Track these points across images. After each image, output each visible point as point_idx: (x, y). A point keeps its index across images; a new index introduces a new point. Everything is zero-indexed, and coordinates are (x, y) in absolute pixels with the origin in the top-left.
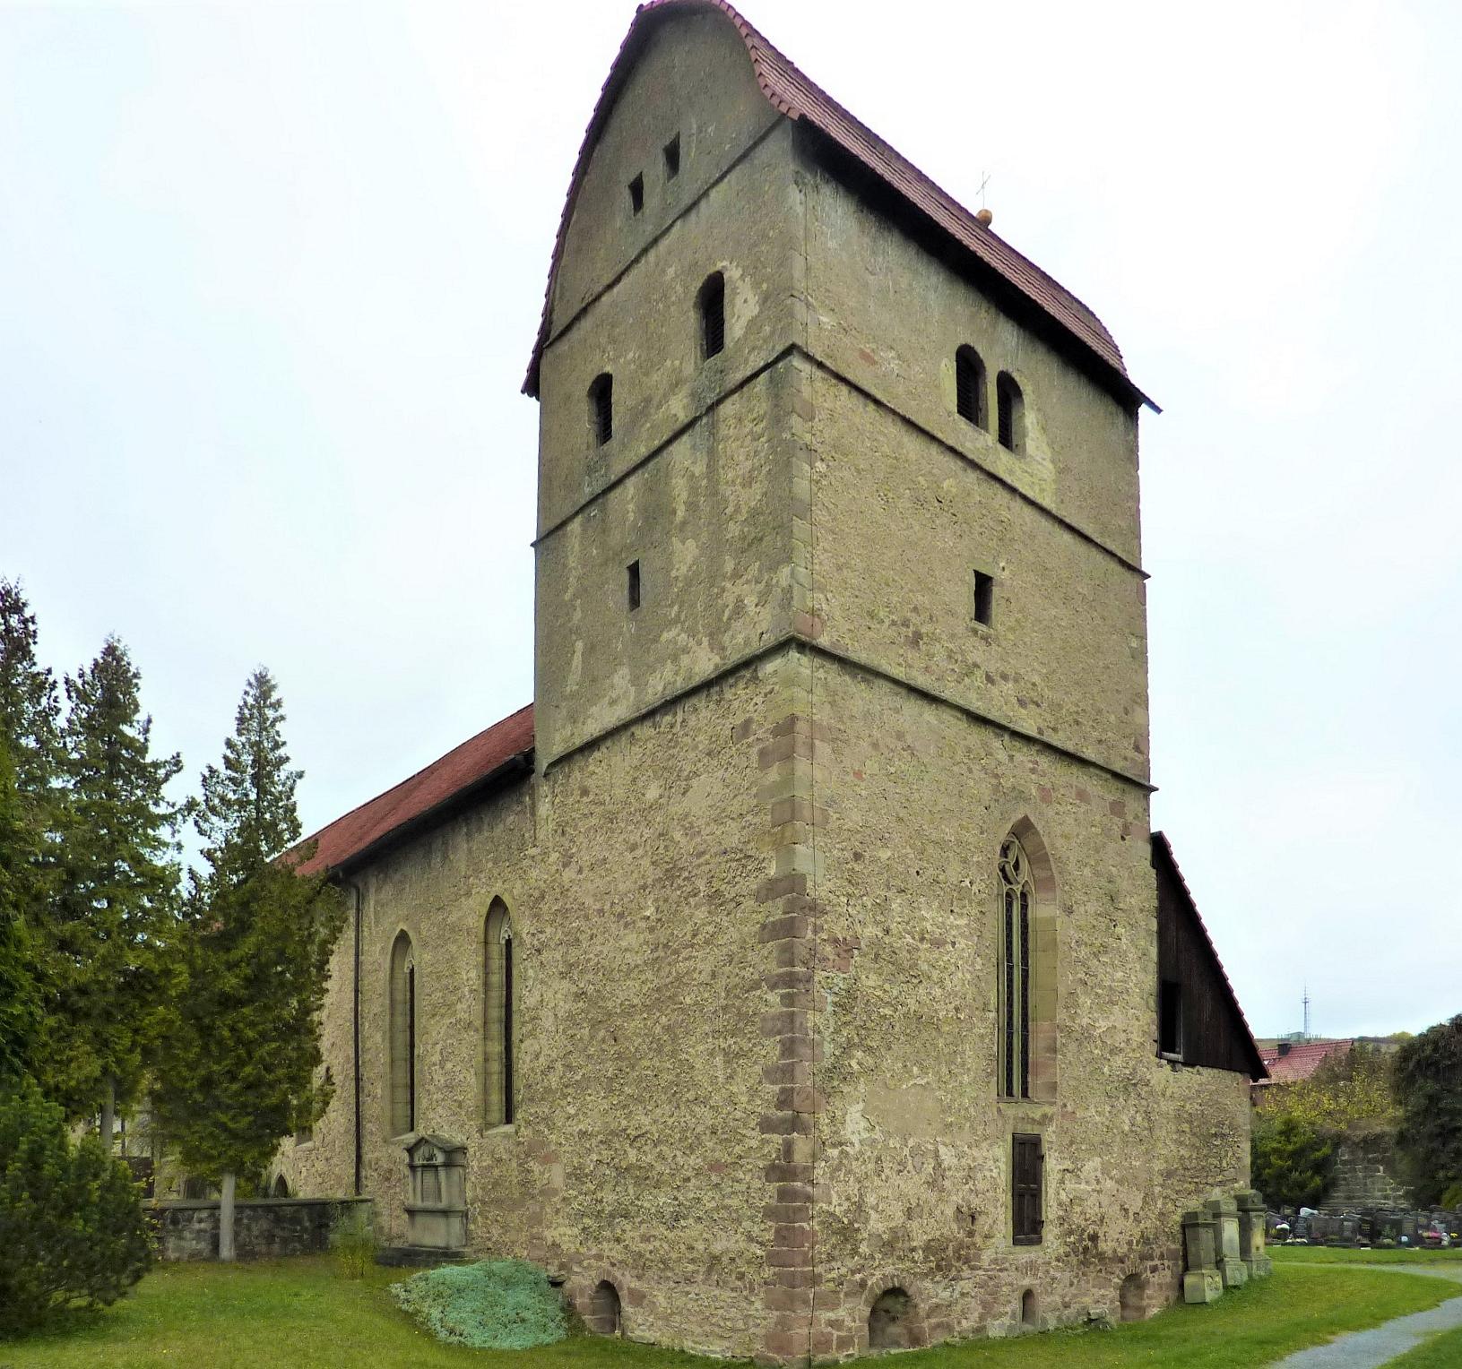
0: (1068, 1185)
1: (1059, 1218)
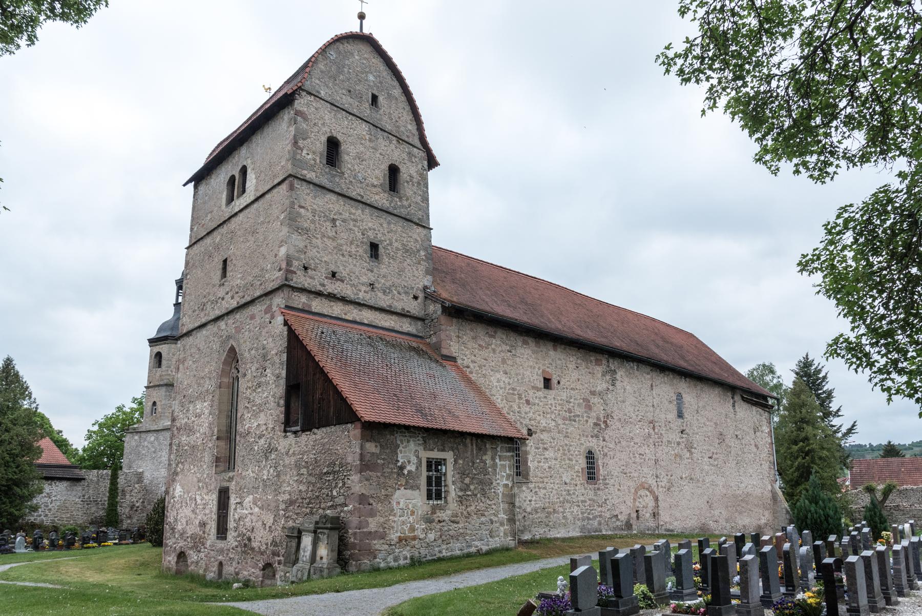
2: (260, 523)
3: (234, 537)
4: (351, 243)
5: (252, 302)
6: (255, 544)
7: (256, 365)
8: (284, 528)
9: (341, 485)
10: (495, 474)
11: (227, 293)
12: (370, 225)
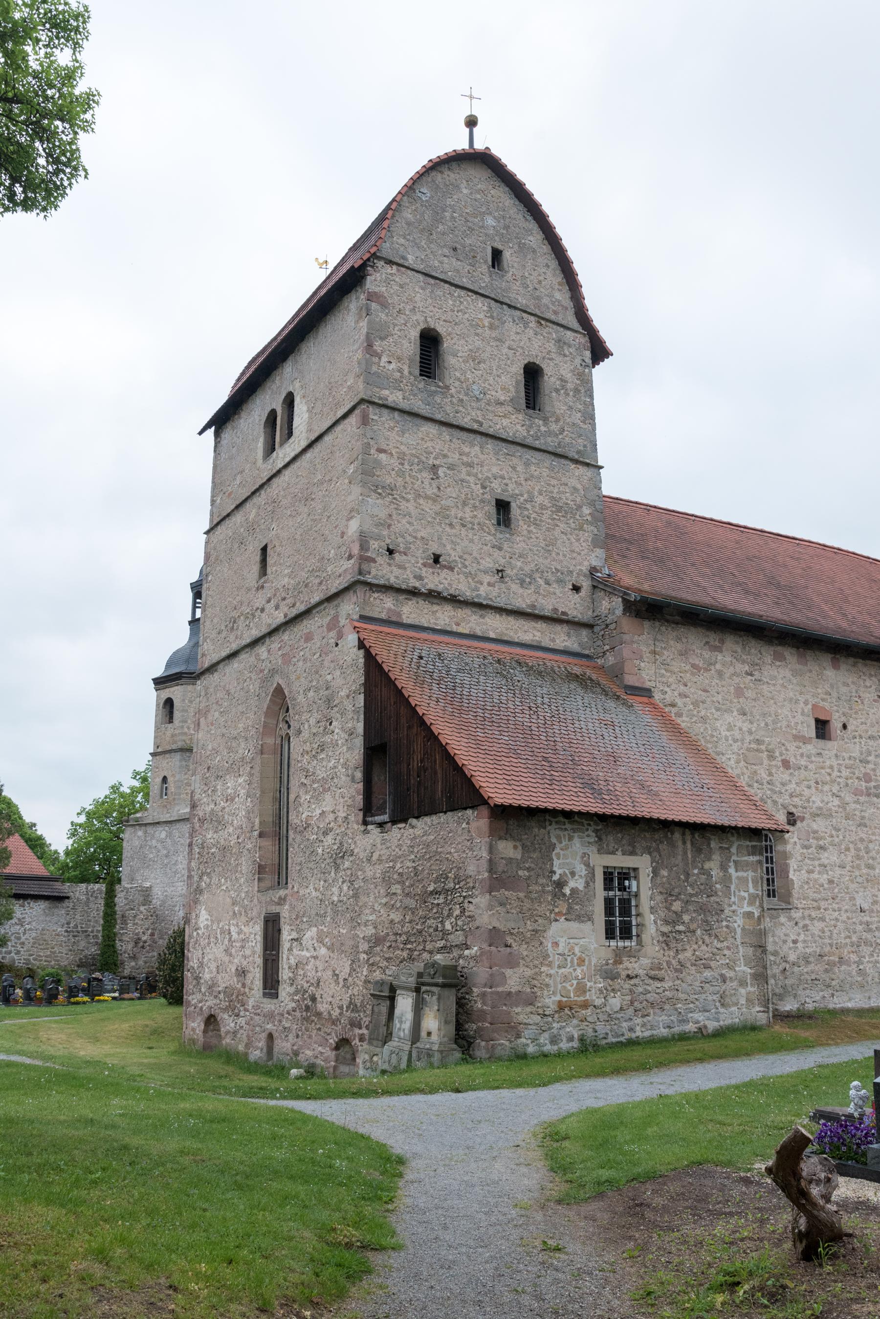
0: (295, 951)
1: (290, 978)
2: (330, 973)
3: (289, 994)
4: (465, 504)
5: (307, 613)
6: (322, 1007)
7: (316, 716)
8: (367, 982)
9: (457, 912)
10: (727, 893)
11: (269, 601)
12: (495, 470)
